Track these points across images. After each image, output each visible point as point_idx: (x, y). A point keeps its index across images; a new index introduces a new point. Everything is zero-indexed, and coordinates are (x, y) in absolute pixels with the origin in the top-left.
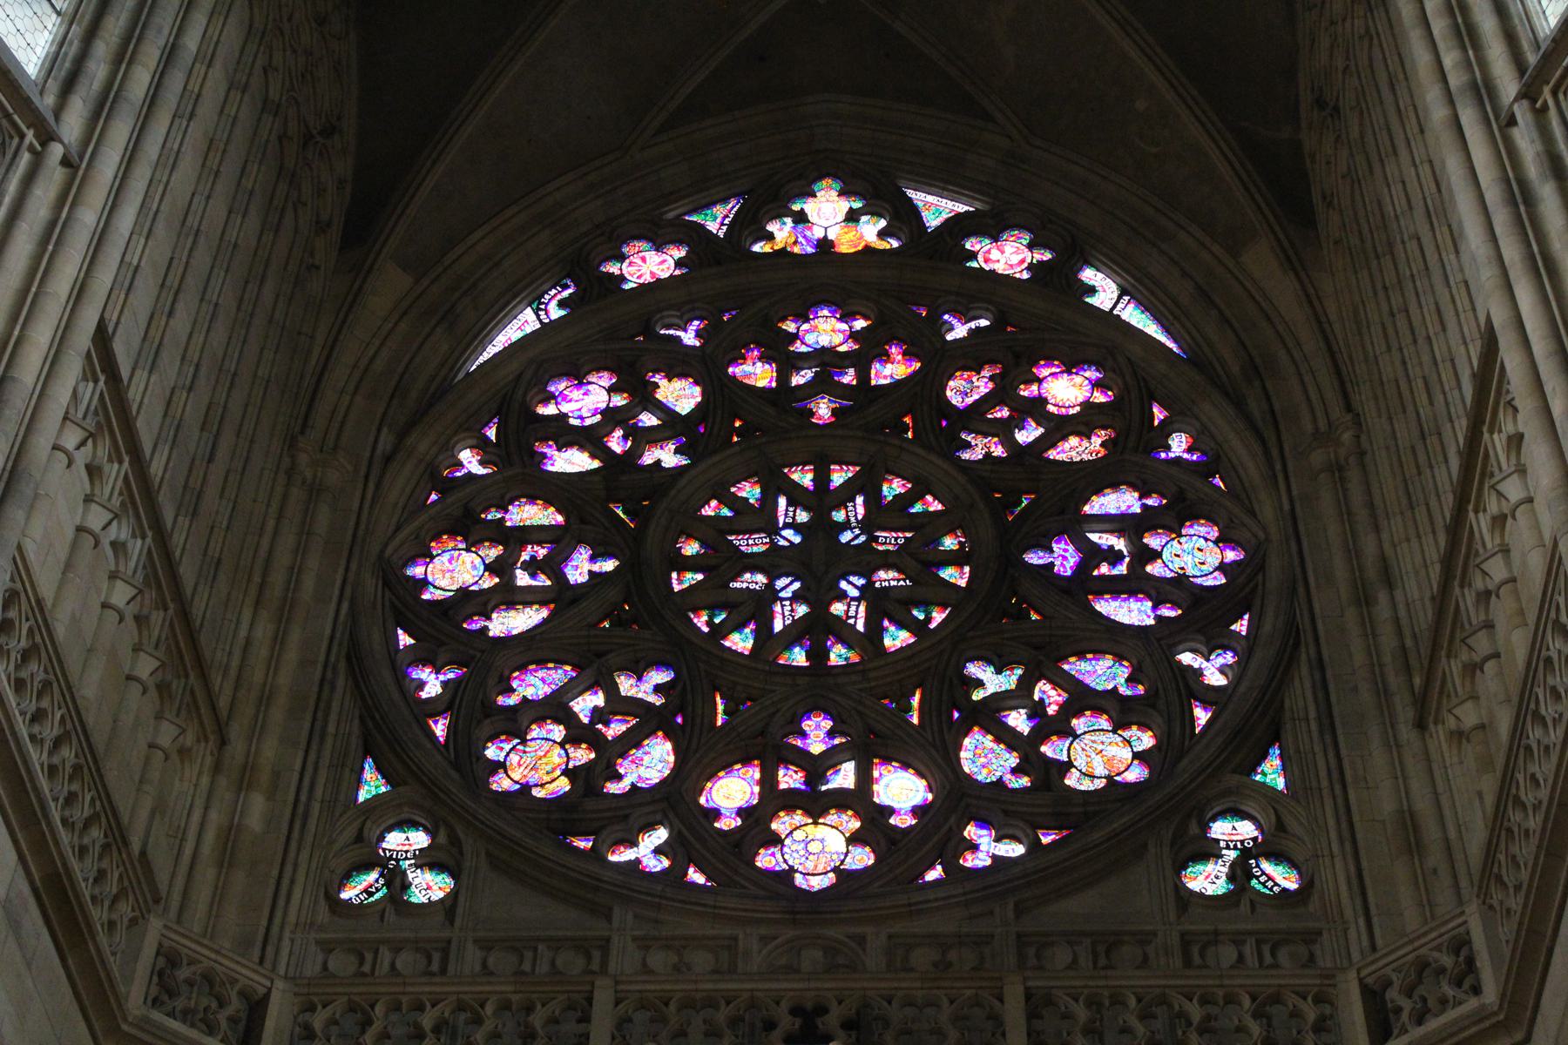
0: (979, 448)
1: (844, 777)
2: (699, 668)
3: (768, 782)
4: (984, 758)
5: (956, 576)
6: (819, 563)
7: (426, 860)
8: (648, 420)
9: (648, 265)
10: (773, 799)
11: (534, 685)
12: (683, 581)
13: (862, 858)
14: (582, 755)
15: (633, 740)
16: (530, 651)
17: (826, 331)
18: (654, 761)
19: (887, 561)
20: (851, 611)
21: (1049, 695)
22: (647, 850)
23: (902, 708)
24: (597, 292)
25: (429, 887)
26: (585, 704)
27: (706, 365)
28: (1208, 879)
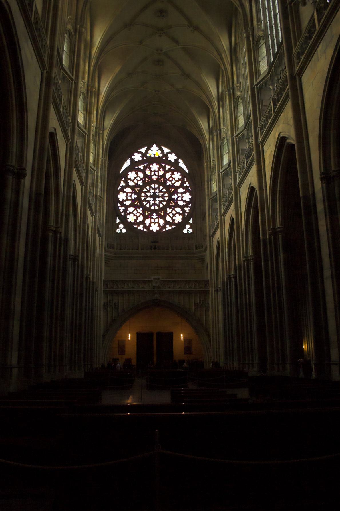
0: (169, 183)
1: (156, 220)
2: (145, 208)
3: (151, 221)
4: (168, 219)
5: (166, 199)
6: (154, 197)
7: (123, 228)
8: (138, 179)
9: (137, 157)
10: (151, 223)
11: (131, 209)
12: (143, 198)
13: (158, 229)
14: (135, 218)
15: (139, 216)
16: (130, 206)
17: (155, 167)
18: (141, 219)
19: (160, 197)
20: (157, 202)
21: (174, 212)
22: (141, 227)
23: (162, 213)
24: (133, 161)
25: (124, 231)
26: (135, 212)
27: (143, 171)
28: (185, 231)
